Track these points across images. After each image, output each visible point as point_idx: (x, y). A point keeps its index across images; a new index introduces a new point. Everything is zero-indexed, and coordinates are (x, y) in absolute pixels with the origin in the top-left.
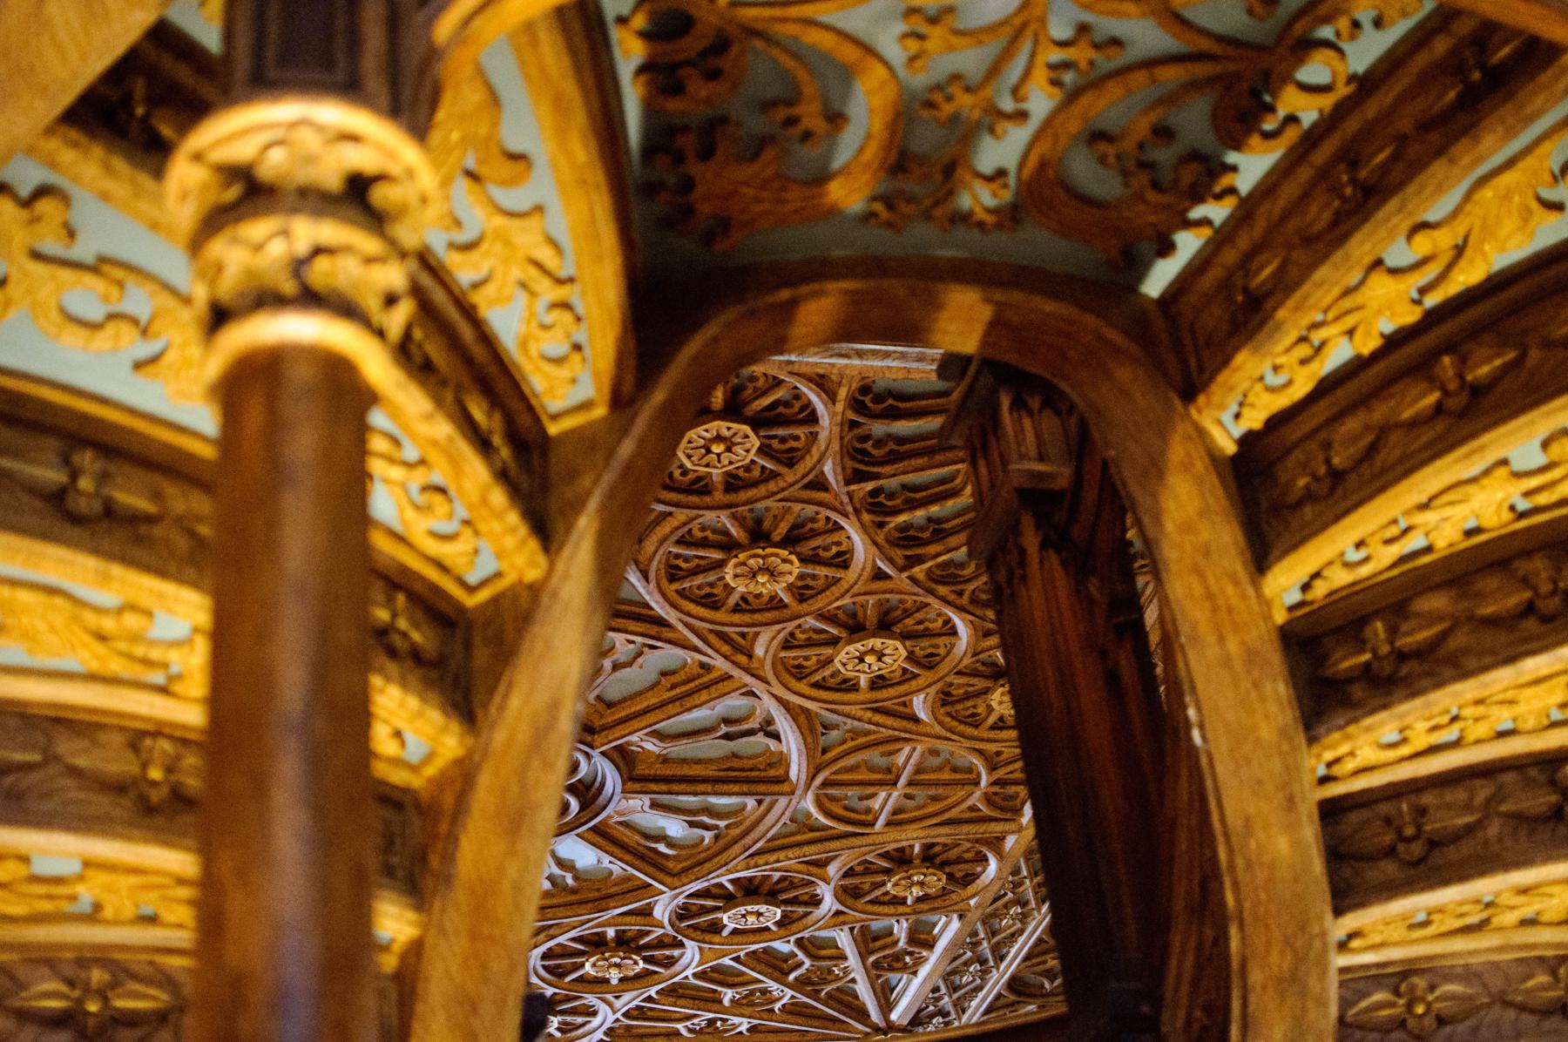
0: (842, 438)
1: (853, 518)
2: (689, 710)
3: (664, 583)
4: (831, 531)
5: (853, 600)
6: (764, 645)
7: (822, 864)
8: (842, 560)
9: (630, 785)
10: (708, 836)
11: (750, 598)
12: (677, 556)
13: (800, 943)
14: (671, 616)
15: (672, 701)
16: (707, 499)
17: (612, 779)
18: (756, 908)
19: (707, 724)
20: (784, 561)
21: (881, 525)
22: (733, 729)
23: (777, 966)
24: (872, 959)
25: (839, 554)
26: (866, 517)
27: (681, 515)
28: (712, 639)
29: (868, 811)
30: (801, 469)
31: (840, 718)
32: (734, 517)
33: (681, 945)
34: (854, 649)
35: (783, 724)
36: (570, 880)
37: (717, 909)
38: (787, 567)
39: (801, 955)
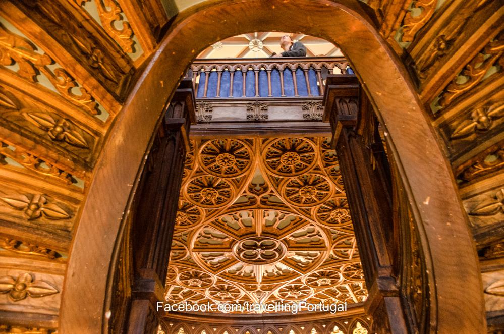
0: (321, 155)
1: (328, 177)
2: (298, 229)
3: (286, 197)
4: (323, 181)
5: (333, 199)
6: (314, 211)
7: (338, 268)
8: (328, 189)
9: (289, 249)
10: (311, 261)
11: (307, 200)
12: (288, 190)
13: (337, 288)
14: (289, 205)
15: (294, 227)
16: (291, 174)
17: (284, 248)
18: (324, 279)
19: (305, 233)
20: (313, 189)
21: (336, 178)
23: (333, 294)
24: (355, 292)
25: (327, 187)
26: (331, 176)
27: (286, 178)
28: (300, 211)
29: (347, 255)
30: (312, 164)
31: (336, 231)
32: (298, 178)
33: (309, 289)
34: (335, 212)
35: (322, 232)
36: (281, 273)
37: (316, 280)
38: (313, 191)
39: (338, 291)
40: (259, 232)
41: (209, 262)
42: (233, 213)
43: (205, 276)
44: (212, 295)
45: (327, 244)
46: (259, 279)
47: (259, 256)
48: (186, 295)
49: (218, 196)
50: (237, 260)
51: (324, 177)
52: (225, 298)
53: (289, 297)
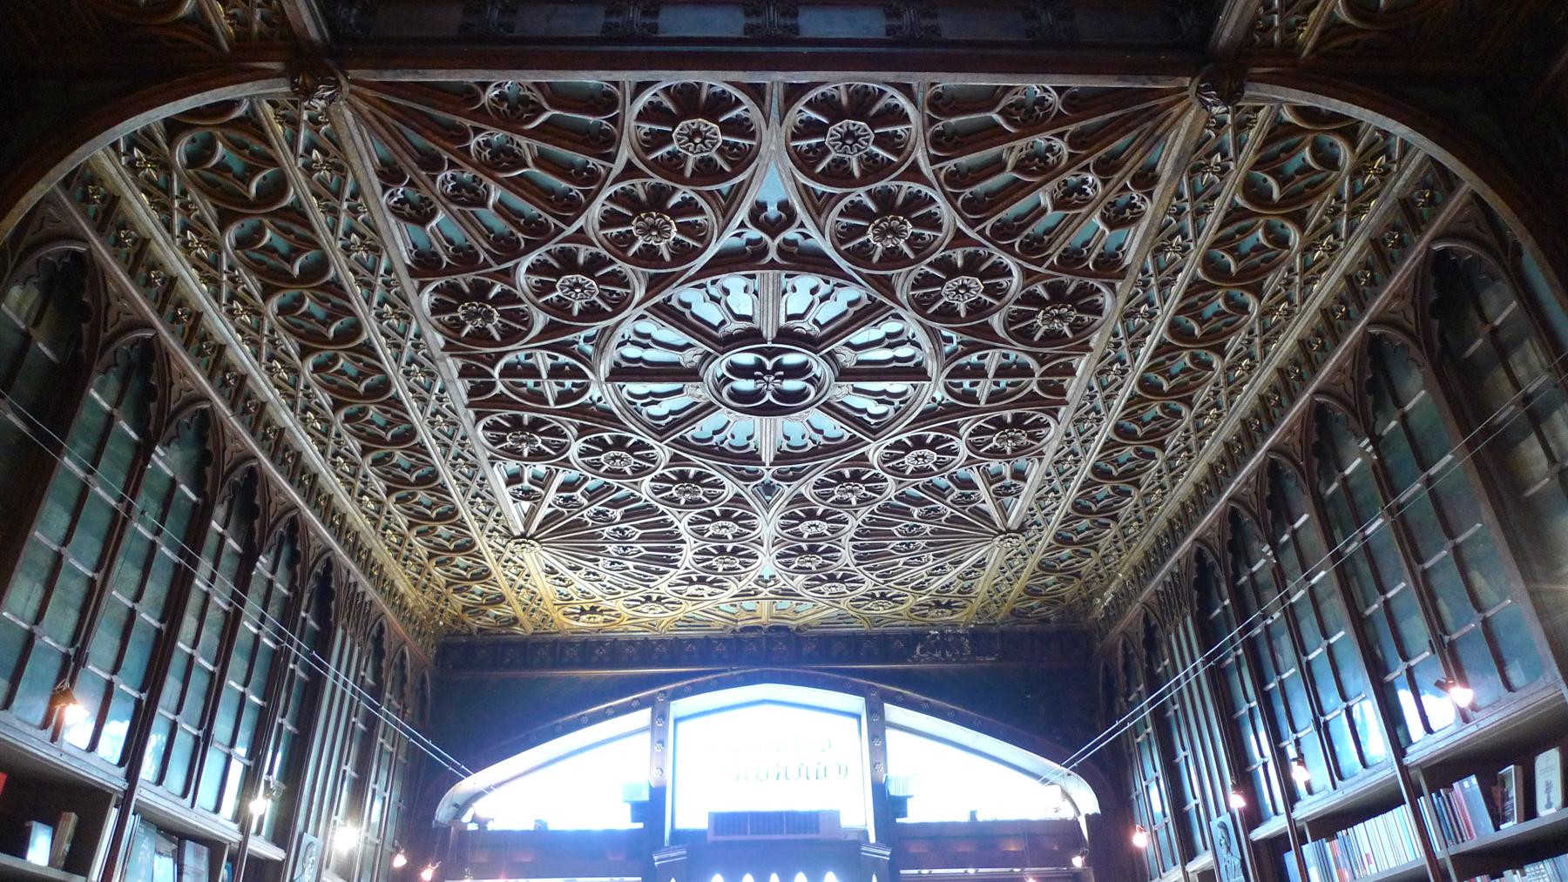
10: (891, 408)
22: (893, 340)
40: (769, 332)
41: (644, 410)
42: (708, 281)
43: (640, 445)
44: (656, 494)
45: (932, 367)
46: (767, 455)
47: (769, 396)
48: (593, 495)
49: (674, 234)
50: (714, 405)
51: (930, 193)
52: (686, 502)
53: (839, 502)
